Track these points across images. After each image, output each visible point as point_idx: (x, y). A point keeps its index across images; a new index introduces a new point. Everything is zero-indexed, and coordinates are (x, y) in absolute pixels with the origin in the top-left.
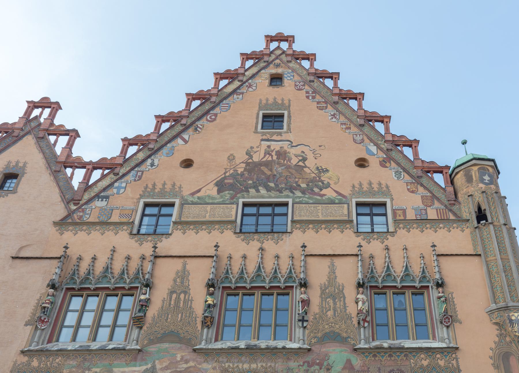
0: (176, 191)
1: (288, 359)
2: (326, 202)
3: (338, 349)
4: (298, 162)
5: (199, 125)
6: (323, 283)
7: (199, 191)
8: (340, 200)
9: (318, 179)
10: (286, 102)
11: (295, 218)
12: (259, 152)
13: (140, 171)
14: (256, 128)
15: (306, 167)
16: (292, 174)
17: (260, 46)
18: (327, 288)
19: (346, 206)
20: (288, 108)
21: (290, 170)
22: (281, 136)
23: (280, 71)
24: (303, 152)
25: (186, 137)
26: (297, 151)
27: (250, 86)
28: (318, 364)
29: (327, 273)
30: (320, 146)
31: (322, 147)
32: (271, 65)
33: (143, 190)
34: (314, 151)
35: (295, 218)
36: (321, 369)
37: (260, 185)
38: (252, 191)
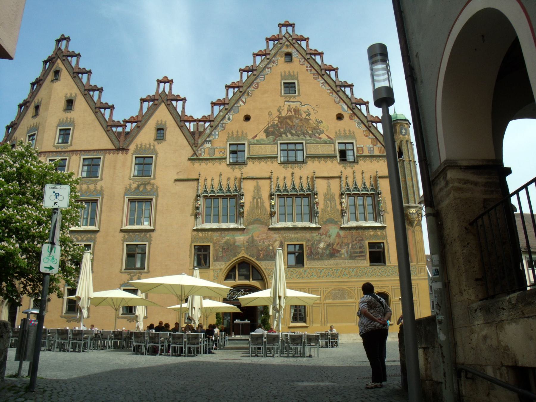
0: (244, 136)
1: (312, 232)
3: (333, 227)
7: (256, 136)
10: (295, 73)
15: (310, 119)
17: (275, 32)
19: (333, 145)
20: (297, 78)
24: (308, 110)
25: (244, 100)
27: (274, 62)
28: (325, 234)
29: (326, 187)
32: (285, 46)
34: (314, 109)
38: (284, 136)
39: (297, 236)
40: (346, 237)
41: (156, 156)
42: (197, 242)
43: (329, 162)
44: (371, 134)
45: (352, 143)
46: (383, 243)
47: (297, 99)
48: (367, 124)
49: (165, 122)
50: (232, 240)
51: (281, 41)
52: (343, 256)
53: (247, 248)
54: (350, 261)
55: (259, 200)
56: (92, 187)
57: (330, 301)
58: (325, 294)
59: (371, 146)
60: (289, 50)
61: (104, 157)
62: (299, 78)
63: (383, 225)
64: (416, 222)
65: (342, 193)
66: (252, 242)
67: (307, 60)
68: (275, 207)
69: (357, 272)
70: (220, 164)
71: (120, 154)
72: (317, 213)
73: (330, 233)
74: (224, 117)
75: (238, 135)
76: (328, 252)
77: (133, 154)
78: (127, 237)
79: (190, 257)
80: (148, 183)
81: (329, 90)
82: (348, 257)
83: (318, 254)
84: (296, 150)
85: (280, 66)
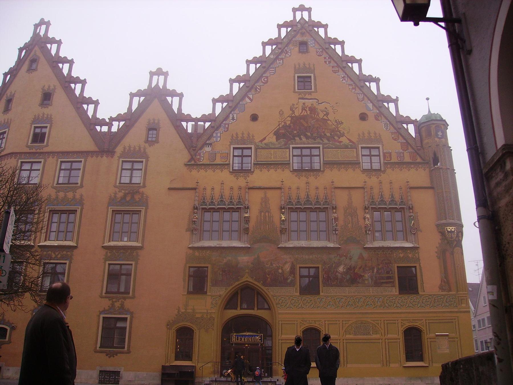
7: (265, 139)
8: (351, 145)
10: (312, 66)
15: (329, 120)
19: (355, 150)
20: (313, 72)
23: (305, 39)
24: (326, 108)
25: (251, 96)
26: (321, 107)
27: (287, 53)
28: (345, 256)
38: (297, 138)
39: (311, 257)
41: (147, 161)
44: (400, 137)
45: (378, 148)
46: (415, 267)
47: (314, 96)
48: (395, 125)
52: (366, 282)
55: (267, 214)
56: (70, 195)
57: (351, 336)
59: (401, 151)
61: (85, 161)
65: (366, 207)
70: (222, 171)
71: (105, 157)
74: (227, 117)
76: (348, 277)
77: (120, 158)
78: (109, 254)
80: (136, 192)
84: (311, 156)
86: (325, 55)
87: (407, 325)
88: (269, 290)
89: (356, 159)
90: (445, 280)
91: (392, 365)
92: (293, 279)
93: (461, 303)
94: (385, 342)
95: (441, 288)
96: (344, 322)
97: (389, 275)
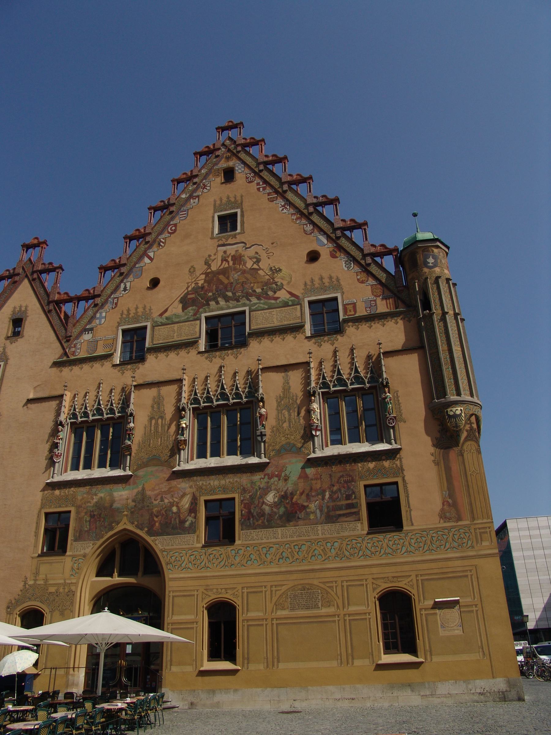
2: (281, 305)
3: (294, 460)
4: (253, 265)
5: (162, 240)
6: (278, 395)
7: (166, 311)
9: (272, 281)
10: (239, 198)
11: (252, 328)
12: (216, 260)
13: (116, 298)
14: (213, 232)
15: (260, 269)
16: (248, 279)
18: (282, 400)
19: (298, 307)
20: (240, 206)
21: (245, 275)
22: (236, 238)
24: (257, 253)
25: (151, 254)
26: (251, 252)
27: (205, 186)
28: (277, 476)
30: (272, 244)
31: (274, 245)
33: (120, 317)
35: (252, 328)
36: (279, 480)
37: (219, 296)
38: (212, 303)
39: (223, 482)
40: (318, 478)
42: (50, 507)
43: (289, 338)
45: (336, 299)
47: (239, 238)
49: (26, 307)
50: (108, 497)
51: (217, 153)
52: (312, 517)
53: (132, 513)
54: (327, 527)
55: (160, 421)
58: (274, 599)
59: (372, 297)
60: (231, 164)
62: (246, 206)
63: (395, 446)
64: (464, 435)
66: (141, 500)
67: (257, 174)
68: (186, 433)
69: (340, 549)
70: (102, 365)
72: (262, 435)
73: (287, 472)
74: (118, 287)
75: (137, 312)
76: (282, 510)
79: (37, 535)
81: (294, 214)
82: (323, 517)
83: (263, 515)
85: (215, 190)
86: (258, 180)
87: (384, 586)
88: (157, 542)
89: (300, 321)
90: (450, 501)
91: (357, 662)
92: (194, 520)
93: (481, 540)
94: (345, 620)
95: (443, 516)
96: (274, 589)
97: (350, 502)
